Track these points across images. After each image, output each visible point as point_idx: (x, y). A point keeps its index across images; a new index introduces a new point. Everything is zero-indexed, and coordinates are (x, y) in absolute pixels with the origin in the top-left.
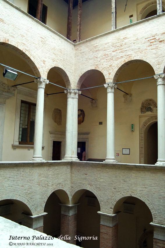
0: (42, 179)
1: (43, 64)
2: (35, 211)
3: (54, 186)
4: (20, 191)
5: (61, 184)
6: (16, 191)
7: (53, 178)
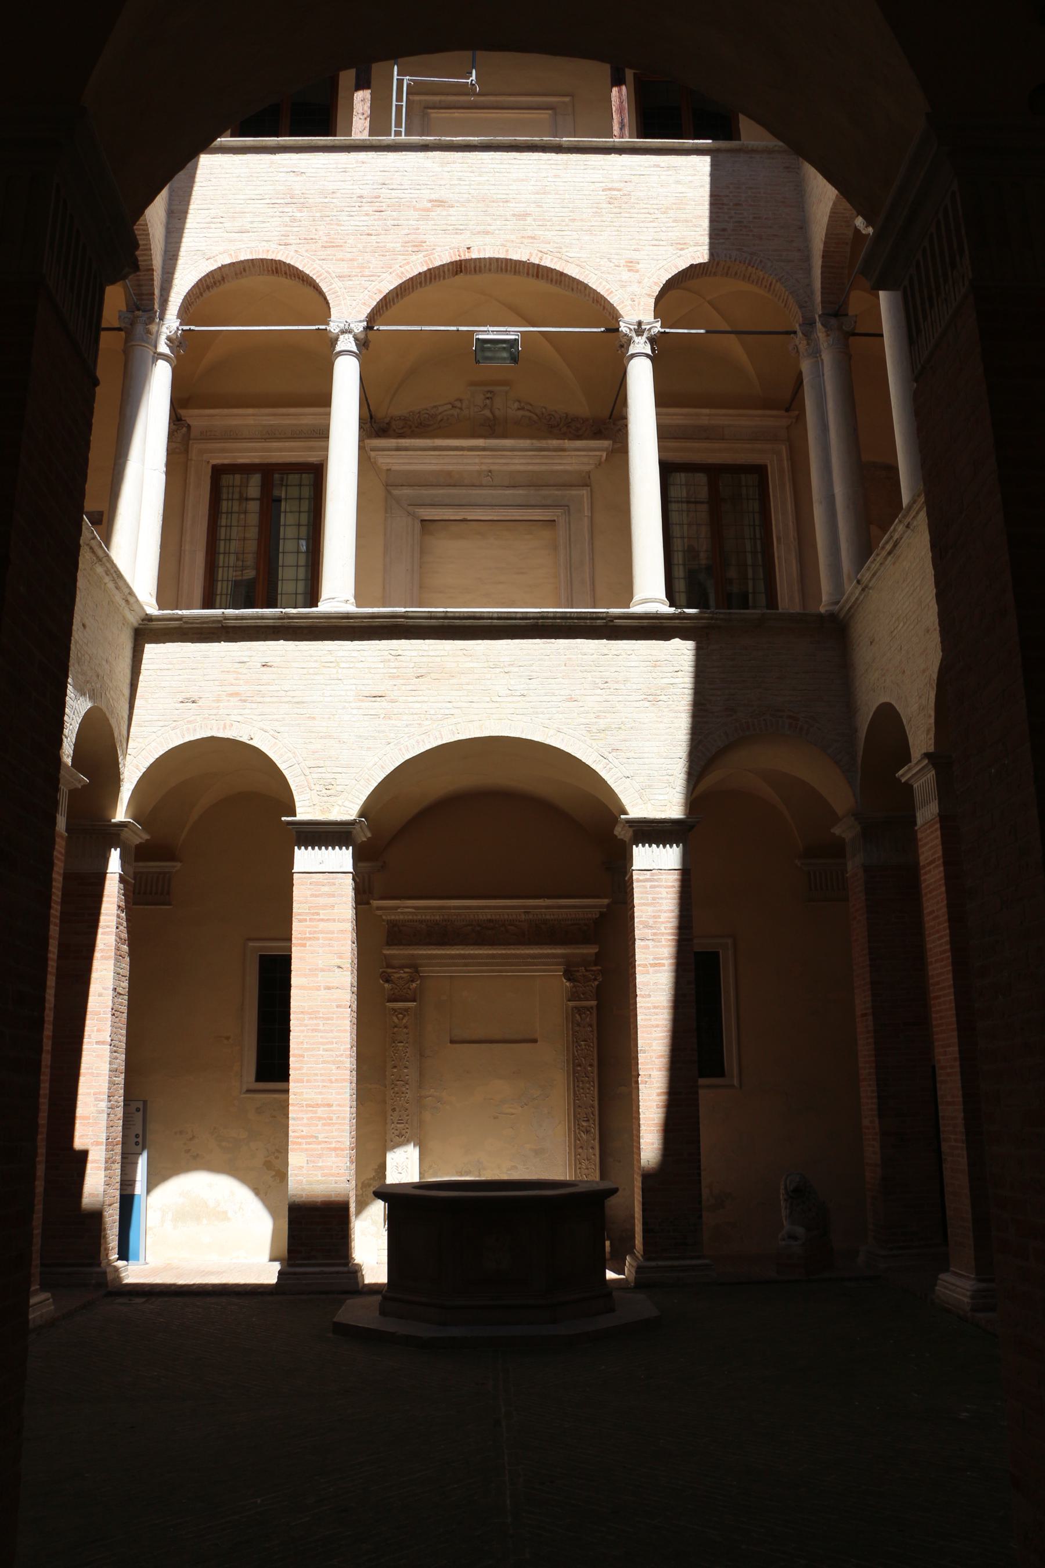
0: (666, 681)
1: (626, 275)
2: (640, 801)
6: (543, 713)
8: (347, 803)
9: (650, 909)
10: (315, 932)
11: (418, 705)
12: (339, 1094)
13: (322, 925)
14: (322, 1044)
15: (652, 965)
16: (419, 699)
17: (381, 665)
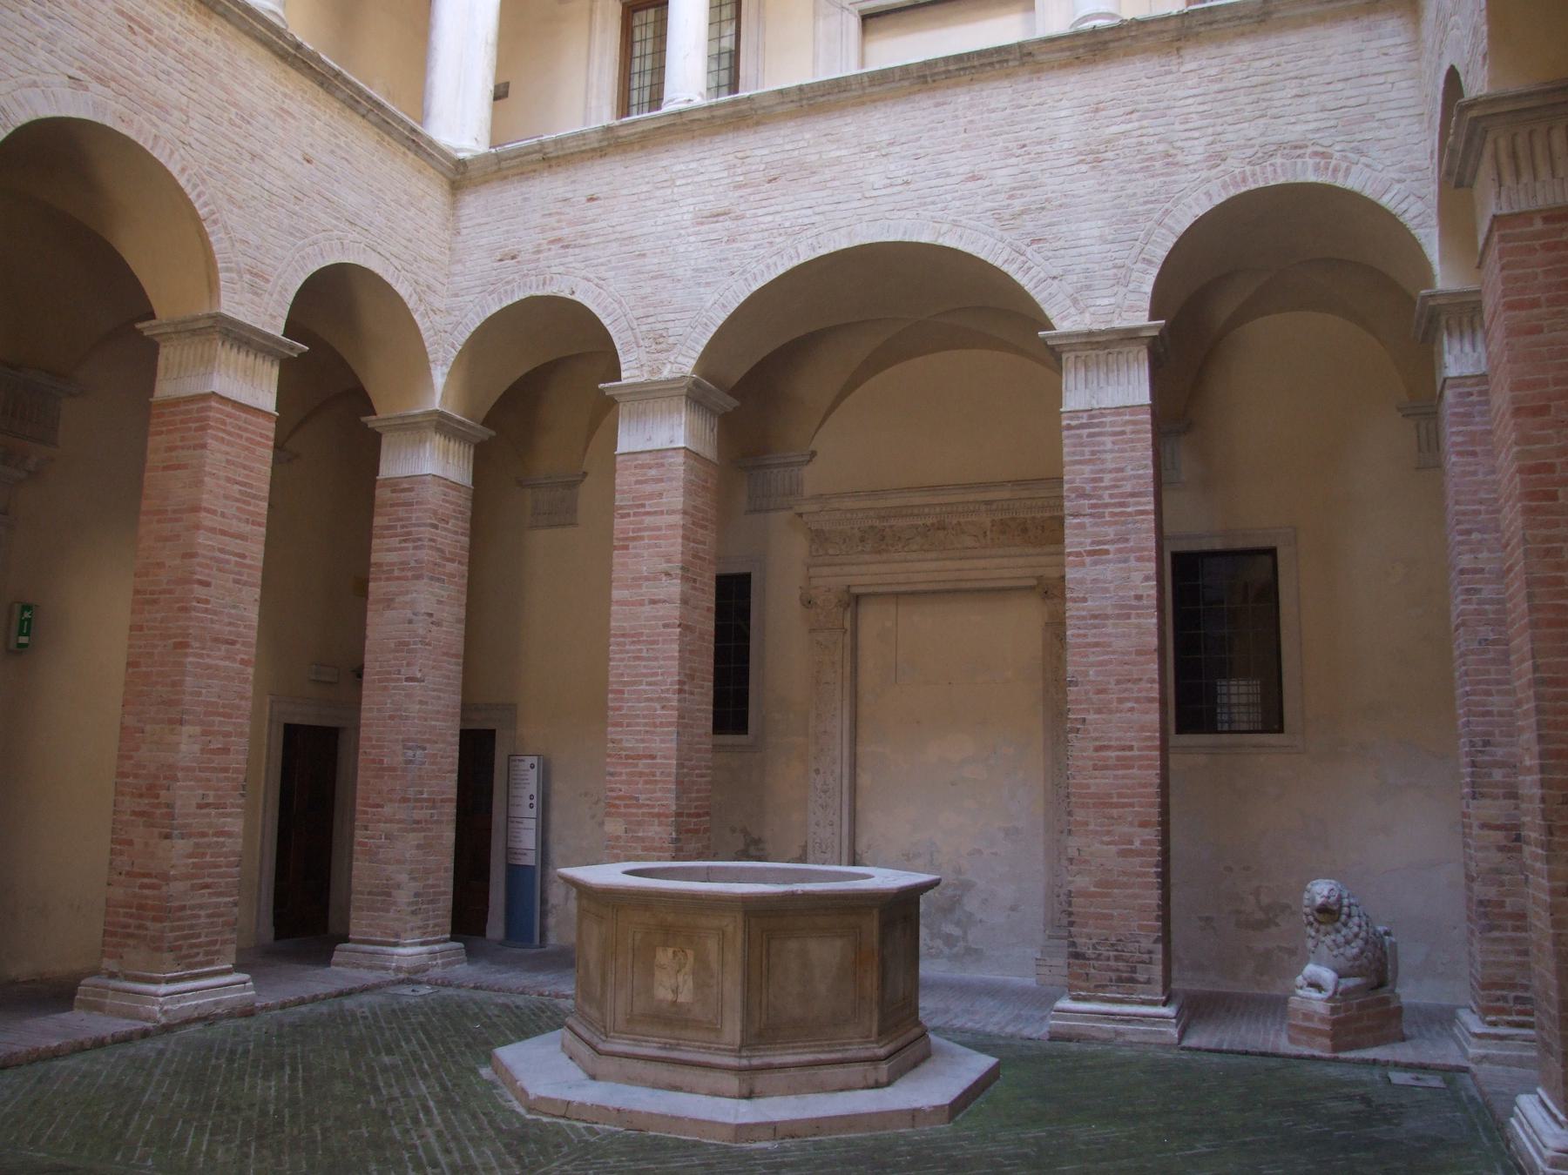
2: (1072, 310)
3: (1234, 165)
4: (958, 203)
5: (1309, 151)
6: (933, 203)
7: (1218, 115)
8: (680, 359)
9: (1087, 468)
10: (639, 530)
11: (770, 218)
12: (662, 741)
13: (648, 520)
14: (645, 675)
15: (1090, 553)
16: (772, 209)
17: (725, 174)
